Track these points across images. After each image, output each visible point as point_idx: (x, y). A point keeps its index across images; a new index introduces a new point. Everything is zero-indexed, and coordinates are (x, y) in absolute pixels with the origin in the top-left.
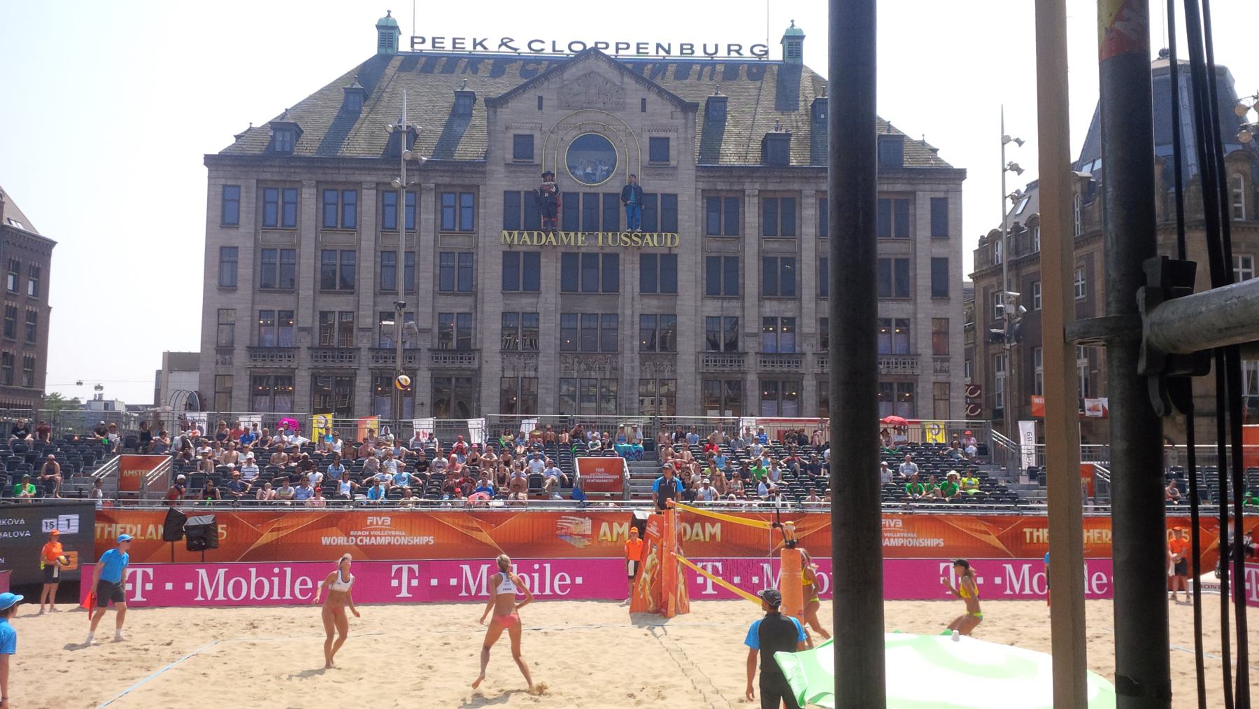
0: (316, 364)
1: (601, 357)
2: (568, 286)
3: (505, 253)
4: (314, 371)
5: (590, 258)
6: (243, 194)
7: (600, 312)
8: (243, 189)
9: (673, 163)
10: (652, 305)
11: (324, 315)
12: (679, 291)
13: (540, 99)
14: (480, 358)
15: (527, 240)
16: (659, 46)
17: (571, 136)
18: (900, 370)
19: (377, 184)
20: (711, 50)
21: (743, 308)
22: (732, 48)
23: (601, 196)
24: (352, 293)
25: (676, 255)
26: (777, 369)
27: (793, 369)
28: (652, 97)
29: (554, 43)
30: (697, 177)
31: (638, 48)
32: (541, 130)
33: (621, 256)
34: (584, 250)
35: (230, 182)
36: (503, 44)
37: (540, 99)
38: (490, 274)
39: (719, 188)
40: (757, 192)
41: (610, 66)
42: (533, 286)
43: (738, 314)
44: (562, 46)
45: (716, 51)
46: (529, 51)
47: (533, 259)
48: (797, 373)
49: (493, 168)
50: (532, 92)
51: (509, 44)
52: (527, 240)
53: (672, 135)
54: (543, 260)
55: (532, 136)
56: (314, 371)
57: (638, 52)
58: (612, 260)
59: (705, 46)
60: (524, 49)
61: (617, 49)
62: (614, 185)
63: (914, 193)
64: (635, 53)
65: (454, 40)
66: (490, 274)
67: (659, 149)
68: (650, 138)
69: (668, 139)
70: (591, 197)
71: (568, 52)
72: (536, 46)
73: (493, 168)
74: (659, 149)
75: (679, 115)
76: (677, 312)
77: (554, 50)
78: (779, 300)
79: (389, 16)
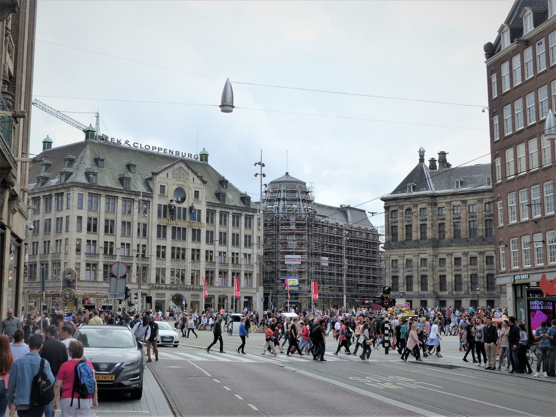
0: (105, 260)
1: (181, 262)
2: (173, 237)
3: (158, 225)
4: (105, 263)
5: (179, 228)
6: (84, 197)
7: (181, 247)
8: (84, 195)
9: (200, 200)
10: (195, 246)
11: (106, 243)
12: (201, 242)
13: (168, 174)
14: (151, 260)
15: (164, 222)
16: (170, 151)
17: (175, 187)
18: (250, 270)
19: (123, 198)
20: (184, 155)
21: (215, 248)
22: (190, 155)
23: (182, 208)
24: (114, 235)
25: (200, 230)
26: (223, 268)
27: (227, 268)
28: (196, 178)
29: (141, 144)
30: (206, 205)
31: (164, 151)
32: (167, 184)
33: (187, 229)
34: (178, 226)
35: (81, 193)
36: (126, 143)
37: (168, 174)
38: (153, 232)
39: (211, 209)
40: (219, 211)
41: (186, 166)
42: (165, 236)
43: (213, 250)
44: (143, 146)
45: (185, 156)
46: (133, 146)
47: (165, 227)
48: (228, 270)
49: (155, 196)
50: (166, 171)
51: (128, 143)
52: (164, 222)
53: (200, 190)
54: (167, 228)
55: (164, 186)
56: (105, 263)
57: (164, 152)
58: (184, 229)
59: (182, 153)
60: (132, 146)
61: (159, 150)
62: (185, 205)
63: (253, 216)
64: (163, 152)
65: (112, 138)
66: (153, 232)
67: (197, 194)
68: (195, 191)
69: (199, 191)
70: (179, 208)
71: (144, 148)
72: (136, 145)
73: (155, 196)
74: (197, 194)
75: (202, 184)
76: (201, 248)
77: (141, 147)
78: (223, 246)
79: (91, 126)
